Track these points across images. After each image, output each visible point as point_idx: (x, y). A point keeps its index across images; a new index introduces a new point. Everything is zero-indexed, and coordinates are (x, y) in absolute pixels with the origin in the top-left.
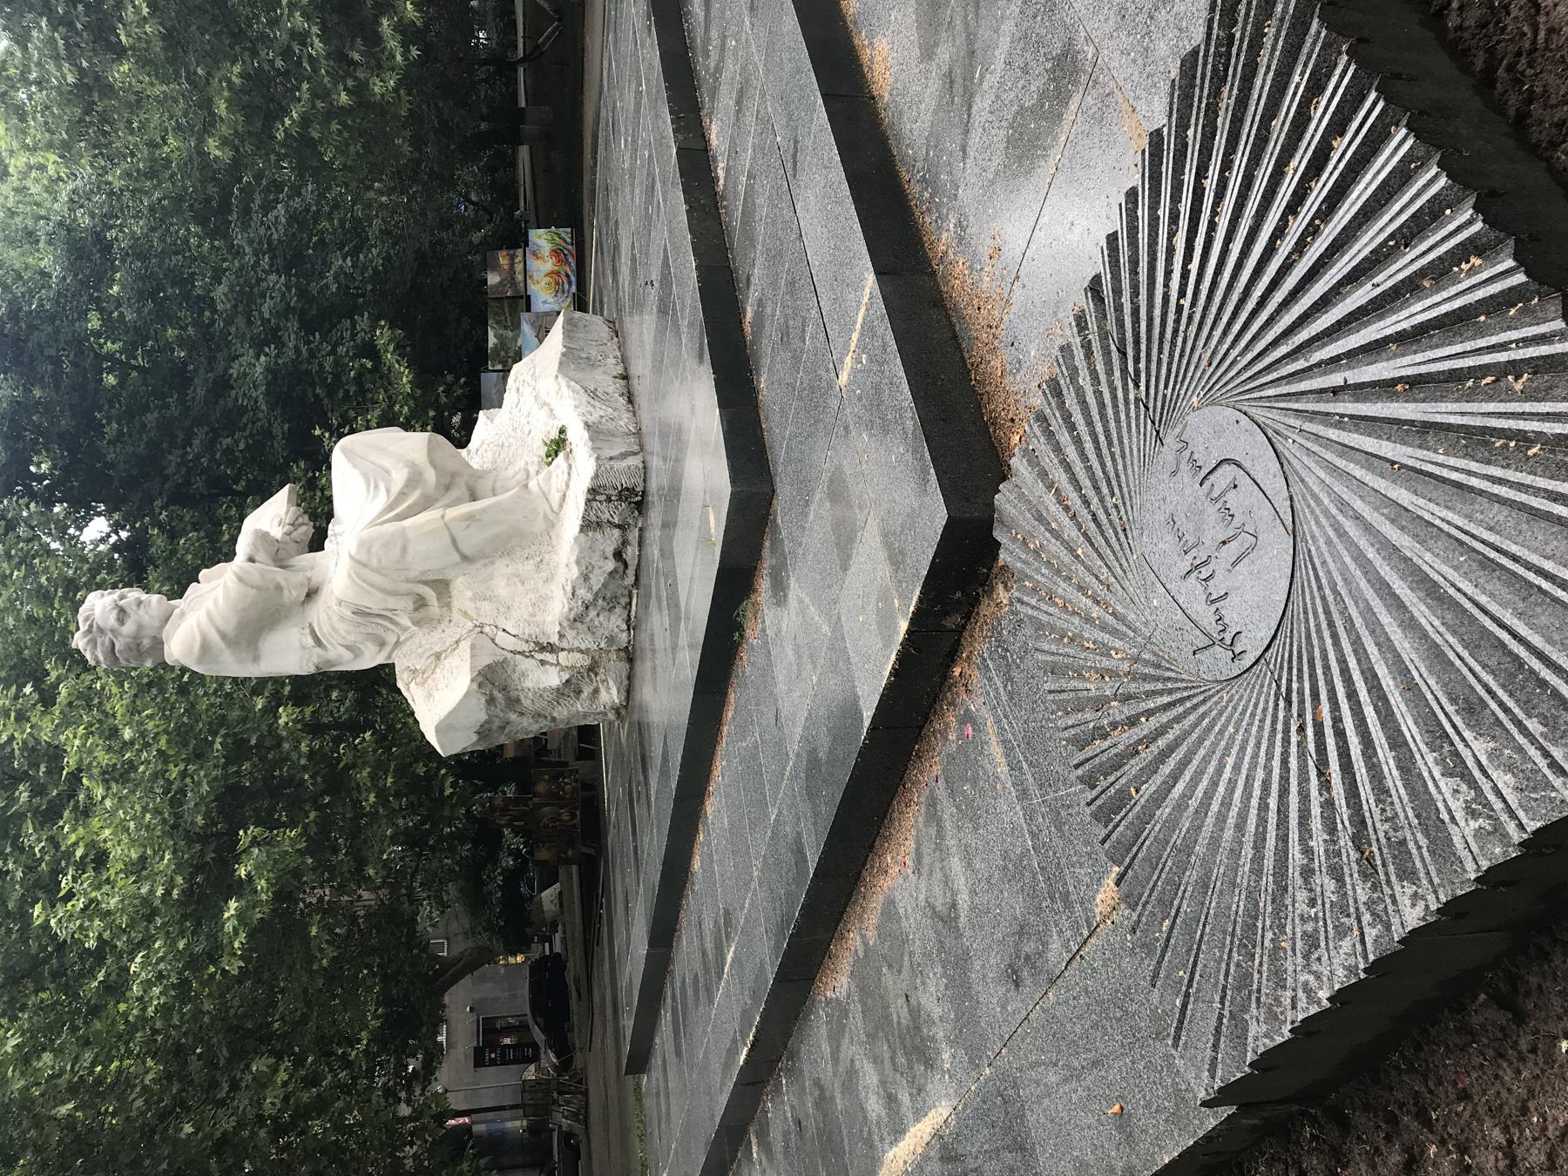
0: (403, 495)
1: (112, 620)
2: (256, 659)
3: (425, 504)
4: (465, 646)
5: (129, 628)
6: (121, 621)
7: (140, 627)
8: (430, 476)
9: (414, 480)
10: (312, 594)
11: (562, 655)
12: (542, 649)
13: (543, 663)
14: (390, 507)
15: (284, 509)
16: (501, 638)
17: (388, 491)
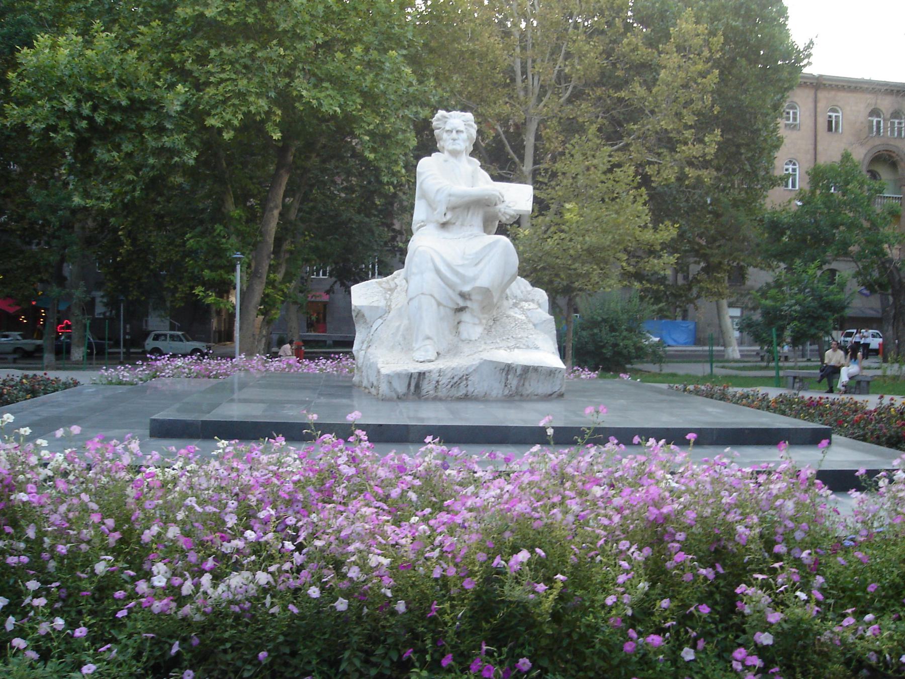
0: (456, 273)
1: (447, 128)
2: (420, 198)
4: (382, 303)
5: (445, 135)
6: (447, 131)
7: (445, 141)
8: (466, 289)
10: (444, 225)
11: (363, 352)
12: (369, 342)
13: (363, 343)
14: (449, 266)
15: (515, 208)
16: (380, 321)
17: (462, 266)
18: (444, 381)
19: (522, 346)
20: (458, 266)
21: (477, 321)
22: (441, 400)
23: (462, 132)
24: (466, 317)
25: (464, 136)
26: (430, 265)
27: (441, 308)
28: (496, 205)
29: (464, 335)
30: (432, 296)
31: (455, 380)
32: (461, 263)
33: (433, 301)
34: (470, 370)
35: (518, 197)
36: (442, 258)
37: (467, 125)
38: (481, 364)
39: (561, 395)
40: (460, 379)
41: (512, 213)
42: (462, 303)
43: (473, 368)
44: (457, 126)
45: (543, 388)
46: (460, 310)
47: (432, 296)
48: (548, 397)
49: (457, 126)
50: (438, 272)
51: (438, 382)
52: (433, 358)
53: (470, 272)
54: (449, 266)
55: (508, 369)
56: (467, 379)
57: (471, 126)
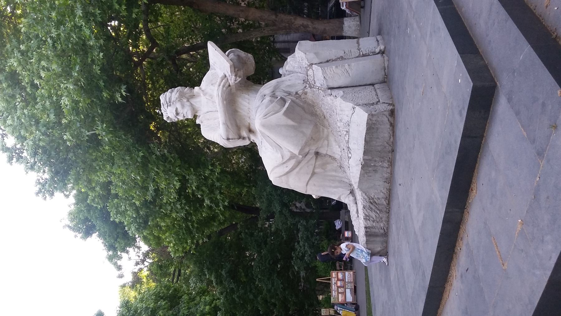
0: (289, 159)
3: (299, 163)
9: (293, 157)
10: (250, 131)
18: (373, 214)
19: (347, 139)
20: (283, 158)
21: (326, 142)
22: (388, 217)
23: (177, 109)
24: (323, 151)
25: (178, 106)
26: (283, 178)
27: (316, 170)
28: (229, 86)
29: (337, 157)
30: (307, 185)
31: (373, 208)
32: (280, 155)
33: (310, 182)
34: (366, 197)
35: (219, 61)
36: (277, 166)
37: (169, 104)
38: (361, 190)
39: (392, 113)
40: (372, 203)
41: (233, 77)
42: (311, 155)
43: (364, 195)
44: (172, 106)
45: (385, 131)
46: (317, 154)
47: (307, 185)
48: (393, 126)
49: (172, 106)
50: (288, 173)
51: (373, 221)
52: (355, 210)
53: (287, 155)
54: (284, 163)
55: (366, 166)
56: (373, 199)
57: (170, 99)
